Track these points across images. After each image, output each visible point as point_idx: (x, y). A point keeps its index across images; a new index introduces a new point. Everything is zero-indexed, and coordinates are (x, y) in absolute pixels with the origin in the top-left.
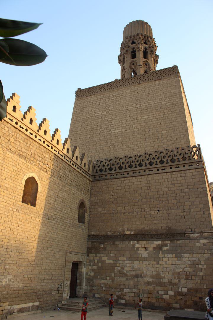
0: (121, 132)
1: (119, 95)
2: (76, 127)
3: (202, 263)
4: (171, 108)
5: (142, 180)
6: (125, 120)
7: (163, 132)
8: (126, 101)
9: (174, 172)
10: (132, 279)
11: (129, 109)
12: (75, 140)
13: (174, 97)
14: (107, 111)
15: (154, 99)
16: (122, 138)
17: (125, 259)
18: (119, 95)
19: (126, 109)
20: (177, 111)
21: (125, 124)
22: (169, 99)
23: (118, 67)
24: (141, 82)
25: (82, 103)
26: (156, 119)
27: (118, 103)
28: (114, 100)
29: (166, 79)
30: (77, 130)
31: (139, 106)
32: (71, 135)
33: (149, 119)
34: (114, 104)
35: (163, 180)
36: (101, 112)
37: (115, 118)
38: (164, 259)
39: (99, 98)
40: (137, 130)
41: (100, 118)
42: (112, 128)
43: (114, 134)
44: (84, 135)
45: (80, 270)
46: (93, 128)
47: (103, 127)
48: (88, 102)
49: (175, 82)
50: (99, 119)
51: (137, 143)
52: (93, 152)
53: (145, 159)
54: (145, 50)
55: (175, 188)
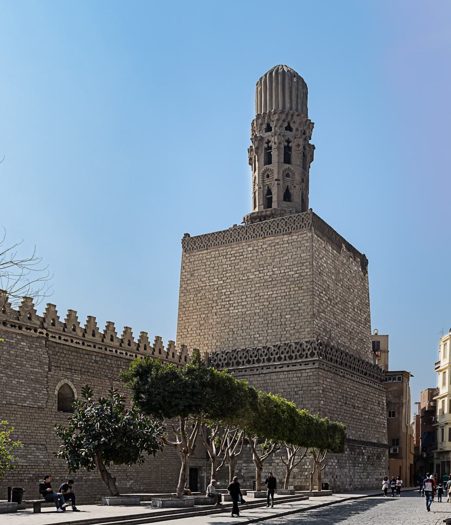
0: (241, 313)
1: (238, 254)
2: (186, 300)
3: (308, 464)
4: (298, 282)
5: (259, 379)
6: (245, 295)
7: (286, 316)
8: (246, 265)
9: (291, 371)
10: (248, 480)
11: (250, 279)
12: (187, 321)
13: (303, 266)
14: (223, 279)
15: (280, 265)
16: (242, 321)
17: (242, 461)
18: (238, 254)
19: (246, 278)
20: (305, 287)
21: (246, 301)
22: (297, 267)
23: (248, 178)
24: (266, 234)
25: (191, 262)
26: (280, 298)
27: (238, 267)
28: (233, 262)
29: (297, 234)
30: (188, 306)
31: (262, 275)
32: (181, 313)
33: (273, 296)
34: (233, 268)
35: (280, 380)
36: (217, 280)
37: (233, 291)
38: (277, 461)
39: (213, 256)
40: (258, 311)
41: (216, 289)
42: (230, 307)
43: (233, 314)
44: (198, 313)
45: (200, 475)
46: (208, 304)
47: (219, 304)
48: (200, 262)
49: (307, 240)
50: (214, 290)
51: (258, 329)
52: (209, 338)
53: (264, 354)
54: (286, 144)
55: (290, 390)
